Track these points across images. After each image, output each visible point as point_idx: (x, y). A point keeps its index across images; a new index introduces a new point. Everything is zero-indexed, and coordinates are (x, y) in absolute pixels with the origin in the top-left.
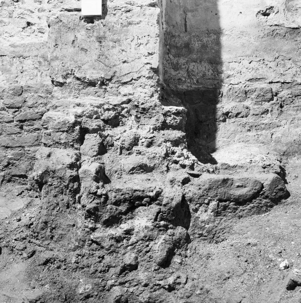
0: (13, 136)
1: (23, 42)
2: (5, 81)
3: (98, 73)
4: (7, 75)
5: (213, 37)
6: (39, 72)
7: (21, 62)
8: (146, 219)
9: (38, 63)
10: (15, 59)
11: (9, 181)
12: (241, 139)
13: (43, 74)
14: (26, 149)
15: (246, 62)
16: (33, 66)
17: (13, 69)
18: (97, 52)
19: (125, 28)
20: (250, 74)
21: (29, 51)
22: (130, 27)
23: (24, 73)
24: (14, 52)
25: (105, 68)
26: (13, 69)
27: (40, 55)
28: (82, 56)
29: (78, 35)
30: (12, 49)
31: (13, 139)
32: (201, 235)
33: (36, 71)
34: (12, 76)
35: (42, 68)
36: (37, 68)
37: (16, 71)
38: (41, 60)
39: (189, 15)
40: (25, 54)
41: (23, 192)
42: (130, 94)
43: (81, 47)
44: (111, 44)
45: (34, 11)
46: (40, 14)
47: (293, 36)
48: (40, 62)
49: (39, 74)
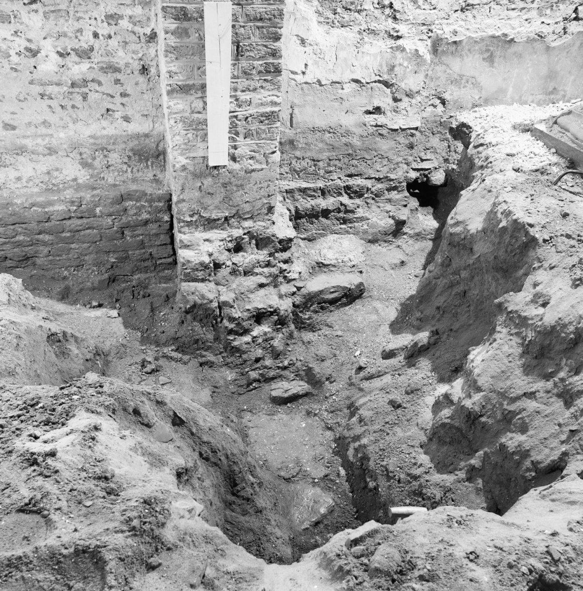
1: (105, 132)
2: (88, 177)
3: (223, 212)
4: (90, 171)
7: (105, 156)
8: (267, 326)
10: (97, 153)
11: (114, 281)
13: (135, 170)
14: (130, 253)
16: (121, 161)
17: (97, 163)
18: (223, 195)
19: (249, 175)
21: (114, 144)
22: (253, 174)
23: (111, 168)
24: (95, 144)
26: (97, 163)
28: (208, 201)
29: (205, 182)
30: (92, 141)
31: (116, 244)
32: (304, 327)
33: (125, 167)
34: (96, 171)
35: (132, 163)
36: (126, 163)
37: (99, 166)
39: (296, 111)
40: (109, 147)
41: (133, 291)
44: (235, 188)
45: (114, 95)
46: (124, 100)
47: (393, 136)
48: (129, 157)
49: (129, 170)
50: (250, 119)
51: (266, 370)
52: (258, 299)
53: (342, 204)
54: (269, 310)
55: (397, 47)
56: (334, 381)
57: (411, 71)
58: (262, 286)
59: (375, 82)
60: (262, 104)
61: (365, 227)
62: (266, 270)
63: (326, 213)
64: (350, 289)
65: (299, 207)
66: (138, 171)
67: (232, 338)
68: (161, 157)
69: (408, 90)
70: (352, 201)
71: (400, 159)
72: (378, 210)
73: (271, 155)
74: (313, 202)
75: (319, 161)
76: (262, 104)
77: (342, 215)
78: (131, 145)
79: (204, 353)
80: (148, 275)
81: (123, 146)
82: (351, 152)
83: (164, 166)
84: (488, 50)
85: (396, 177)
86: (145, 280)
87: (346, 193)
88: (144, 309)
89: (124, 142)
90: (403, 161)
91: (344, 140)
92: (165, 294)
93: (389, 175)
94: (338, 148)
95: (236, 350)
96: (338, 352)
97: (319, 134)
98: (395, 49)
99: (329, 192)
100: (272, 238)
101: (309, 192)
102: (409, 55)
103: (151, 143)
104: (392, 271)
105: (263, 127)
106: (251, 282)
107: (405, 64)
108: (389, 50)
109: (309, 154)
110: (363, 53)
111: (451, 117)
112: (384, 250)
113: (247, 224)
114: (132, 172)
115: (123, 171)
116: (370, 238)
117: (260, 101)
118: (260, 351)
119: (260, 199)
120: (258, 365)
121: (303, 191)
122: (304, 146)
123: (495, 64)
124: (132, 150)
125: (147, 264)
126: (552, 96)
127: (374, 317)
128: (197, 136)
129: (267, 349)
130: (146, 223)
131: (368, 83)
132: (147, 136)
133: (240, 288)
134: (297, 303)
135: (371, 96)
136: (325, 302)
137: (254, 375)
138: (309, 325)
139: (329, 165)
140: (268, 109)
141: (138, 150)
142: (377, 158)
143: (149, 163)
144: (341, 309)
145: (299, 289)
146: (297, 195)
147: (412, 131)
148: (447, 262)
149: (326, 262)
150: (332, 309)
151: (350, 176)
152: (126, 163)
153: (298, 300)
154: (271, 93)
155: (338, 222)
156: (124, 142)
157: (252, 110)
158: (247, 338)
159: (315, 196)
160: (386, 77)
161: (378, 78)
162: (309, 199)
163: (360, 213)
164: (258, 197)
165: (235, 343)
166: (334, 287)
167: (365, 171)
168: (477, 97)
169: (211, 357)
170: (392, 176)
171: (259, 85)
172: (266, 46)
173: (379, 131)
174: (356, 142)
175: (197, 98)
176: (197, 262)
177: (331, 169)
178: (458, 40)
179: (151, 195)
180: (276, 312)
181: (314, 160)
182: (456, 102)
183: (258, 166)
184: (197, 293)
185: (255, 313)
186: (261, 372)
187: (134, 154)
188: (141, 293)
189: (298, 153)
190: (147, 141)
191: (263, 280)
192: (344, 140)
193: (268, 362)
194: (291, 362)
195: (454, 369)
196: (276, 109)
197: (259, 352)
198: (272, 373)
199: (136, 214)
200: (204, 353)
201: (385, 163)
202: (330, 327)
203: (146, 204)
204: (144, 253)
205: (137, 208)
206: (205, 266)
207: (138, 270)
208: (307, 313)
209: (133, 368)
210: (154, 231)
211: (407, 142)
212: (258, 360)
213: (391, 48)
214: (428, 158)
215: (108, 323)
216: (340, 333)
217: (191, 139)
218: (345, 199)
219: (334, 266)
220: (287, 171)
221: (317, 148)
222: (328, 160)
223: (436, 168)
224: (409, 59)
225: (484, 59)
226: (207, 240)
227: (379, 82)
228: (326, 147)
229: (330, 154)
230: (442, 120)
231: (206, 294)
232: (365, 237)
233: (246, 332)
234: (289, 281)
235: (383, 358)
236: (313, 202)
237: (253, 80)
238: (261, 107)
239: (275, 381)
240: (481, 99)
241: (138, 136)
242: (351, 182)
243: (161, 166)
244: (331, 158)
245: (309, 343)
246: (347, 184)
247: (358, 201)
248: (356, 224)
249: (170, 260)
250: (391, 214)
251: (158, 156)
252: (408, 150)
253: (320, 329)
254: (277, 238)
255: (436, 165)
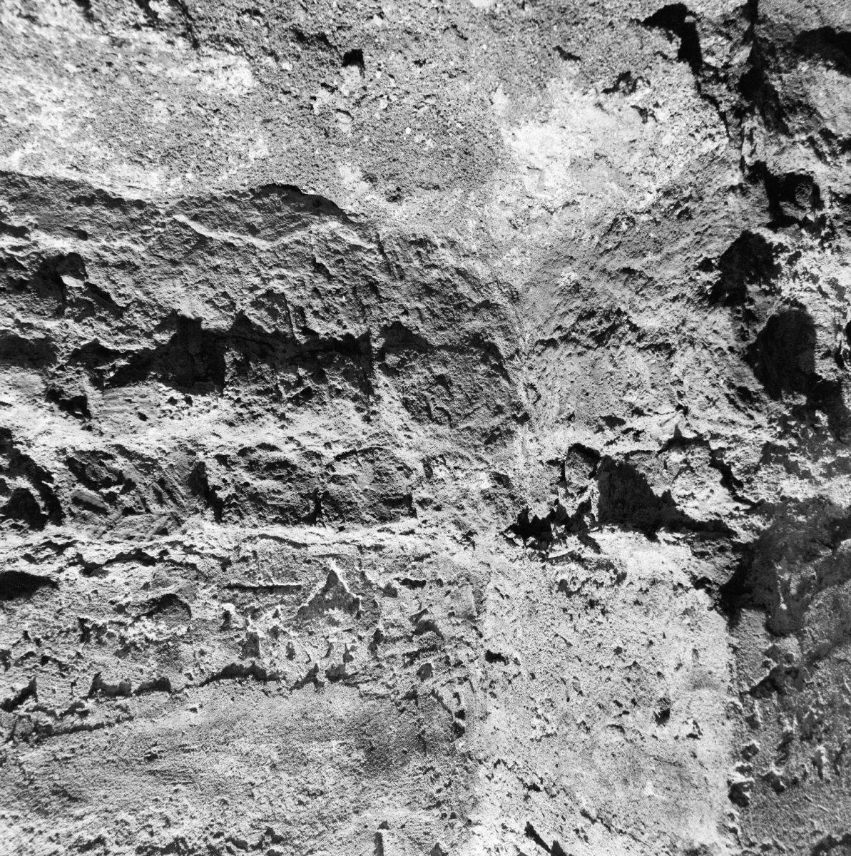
5: (244, 825)
12: (124, 218)
15: (54, 693)
20: (26, 626)
53: (76, 407)
63: (193, 360)
65: (357, 418)
75: (231, 672)
77: (77, 332)
82: (33, 756)
87: (40, 476)
94: (125, 764)
99: (164, 492)
101: (290, 496)
109: (287, 706)
121: (324, 506)
122: (314, 750)
146: (358, 480)
159: (252, 466)
162: (289, 453)
177: (148, 628)
181: (260, 676)
189: (341, 702)
220: (388, 603)
221: (244, 745)
222: (178, 681)
228: (196, 760)
244: (161, 697)
246: (36, 538)
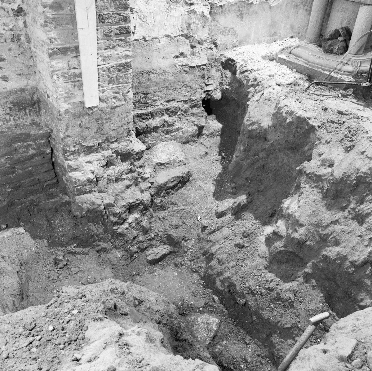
0: (10, 175)
6: (12, 116)
9: (8, 109)
13: (16, 118)
15: (165, 91)
19: (113, 110)
22: (116, 109)
25: (101, 136)
27: (9, 102)
28: (86, 133)
29: (83, 120)
31: (10, 177)
33: (8, 117)
36: (8, 114)
38: (11, 106)
42: (116, 148)
43: (85, 127)
44: (104, 121)
48: (11, 109)
49: (12, 119)
50: (111, 69)
51: (141, 244)
52: (128, 196)
53: (165, 121)
54: (137, 202)
55: (191, 11)
56: (188, 239)
57: (200, 26)
58: (128, 187)
59: (179, 36)
60: (119, 58)
61: (181, 134)
62: (129, 175)
63: (155, 129)
64: (183, 177)
66: (19, 118)
67: (116, 228)
68: (36, 105)
69: (199, 40)
70: (171, 118)
71: (197, 86)
72: (187, 122)
73: (127, 94)
74: (147, 123)
75: (147, 94)
76: (119, 58)
77: (165, 128)
78: (11, 99)
79: (99, 243)
80: (38, 196)
81: (5, 101)
82: (167, 85)
83: (39, 112)
84: (239, 10)
85: (196, 98)
86: (36, 200)
87: (166, 113)
88: (42, 221)
89: (5, 97)
90: (199, 87)
91: (163, 77)
92: (54, 207)
93: (191, 97)
94: (159, 84)
95: (121, 235)
96: (185, 220)
97: (146, 75)
98: (190, 12)
99: (156, 114)
100: (132, 152)
101: (143, 116)
102: (199, 16)
103: (27, 96)
104: (201, 160)
105: (121, 75)
106: (120, 186)
107: (197, 22)
108: (186, 13)
109: (141, 90)
110: (171, 16)
111: (221, 55)
112: (193, 147)
113: (114, 145)
114: (14, 120)
115: (7, 120)
116: (184, 140)
117: (118, 56)
118: (135, 232)
119: (122, 126)
120: (135, 242)
122: (137, 85)
123: (244, 19)
124: (12, 103)
125: (36, 187)
126: (274, 37)
127: (201, 192)
128: (74, 86)
129: (139, 229)
130: (32, 157)
131: (175, 37)
132: (23, 90)
133: (115, 192)
134: (153, 193)
135: (178, 46)
136: (169, 189)
137: (134, 249)
138: (161, 206)
139: (154, 96)
140: (124, 61)
141: (17, 102)
142: (184, 87)
143: (27, 111)
144: (179, 191)
145: (152, 183)
147: (203, 67)
148: (248, 149)
149: (162, 162)
150: (173, 192)
151: (168, 101)
152: (8, 114)
153: (153, 191)
154: (124, 49)
155: (164, 134)
156: (5, 97)
157: (113, 63)
158: (126, 225)
160: (186, 32)
161: (181, 33)
162: (144, 121)
163: (177, 125)
164: (121, 125)
165: (119, 231)
166: (173, 178)
167: (177, 97)
168: (235, 41)
169: (103, 245)
170: (194, 98)
171: (116, 44)
172: (119, 14)
173: (184, 69)
174: (170, 78)
175: (73, 57)
176: (85, 179)
177: (156, 98)
178: (222, 4)
179: (34, 135)
180: (142, 203)
181: (144, 94)
182: (223, 45)
183: (119, 103)
184: (89, 202)
185: (128, 207)
186: (138, 246)
187: (14, 106)
188: (35, 210)
190: (24, 94)
191: (129, 183)
192: (163, 77)
193: (141, 238)
194: (156, 234)
195: (271, 215)
196: (129, 60)
197: (135, 233)
198: (145, 245)
199: (24, 152)
200: (99, 243)
201: (189, 90)
202: (175, 204)
203: (32, 143)
204: (33, 180)
205: (25, 147)
206: (90, 181)
207: (32, 193)
208: (159, 199)
209: (49, 267)
210: (39, 162)
211: (201, 74)
212: (134, 238)
213: (188, 12)
214: (210, 83)
215: (20, 239)
216: (183, 207)
217: (71, 89)
218: (166, 117)
219: (168, 164)
221: (146, 85)
222: (153, 93)
223: (215, 89)
224: (199, 19)
225: (237, 16)
226: (89, 162)
227: (182, 35)
229: (155, 88)
230: (216, 58)
231: (95, 201)
232: (181, 140)
233: (125, 220)
234: (144, 179)
235: (218, 218)
236: (147, 123)
237: (112, 40)
238: (118, 60)
239: (148, 249)
240: (238, 42)
241: (16, 92)
242: (169, 105)
243: (36, 112)
244: (155, 91)
245: (163, 218)
246: (167, 107)
247: (174, 118)
248: (175, 133)
249: (54, 181)
250: (195, 123)
251: (34, 104)
252: (202, 80)
253: (169, 208)
254: (135, 152)
255: (215, 87)
